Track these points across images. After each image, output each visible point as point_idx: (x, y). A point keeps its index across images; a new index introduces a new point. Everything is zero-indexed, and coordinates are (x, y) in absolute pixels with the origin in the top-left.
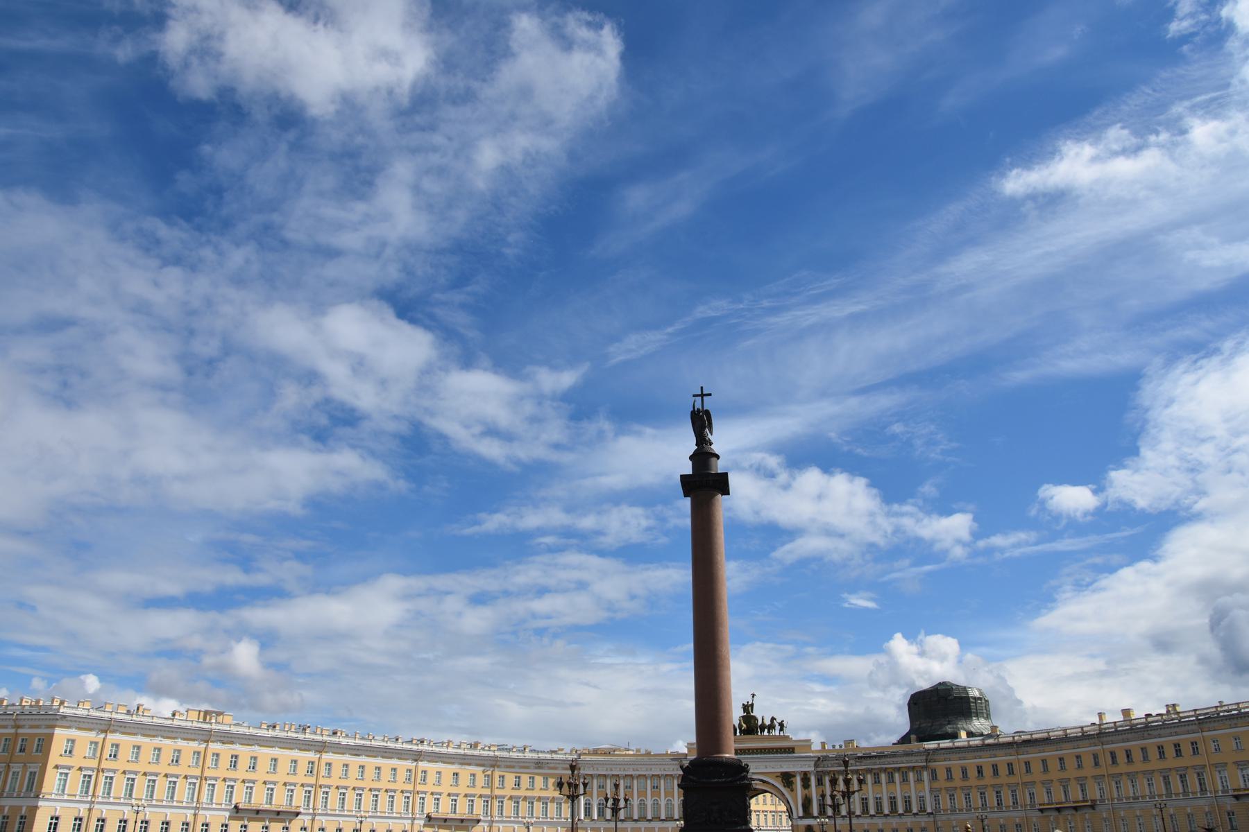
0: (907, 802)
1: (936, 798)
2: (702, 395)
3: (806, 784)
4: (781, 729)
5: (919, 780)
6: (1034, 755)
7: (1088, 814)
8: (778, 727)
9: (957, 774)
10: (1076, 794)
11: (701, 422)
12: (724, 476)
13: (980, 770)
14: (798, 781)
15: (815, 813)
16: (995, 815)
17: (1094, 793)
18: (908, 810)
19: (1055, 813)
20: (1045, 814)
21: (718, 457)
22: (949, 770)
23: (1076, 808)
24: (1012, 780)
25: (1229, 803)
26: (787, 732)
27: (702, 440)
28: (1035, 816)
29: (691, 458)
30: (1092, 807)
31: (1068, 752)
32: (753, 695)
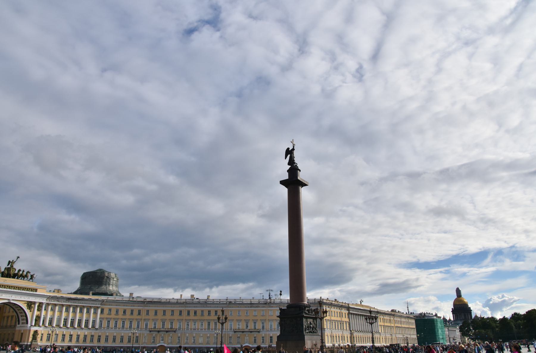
0: (87, 322)
3: (39, 309)
4: (32, 278)
6: (152, 308)
7: (171, 334)
8: (30, 277)
9: (113, 312)
10: (168, 326)
11: (289, 152)
13: (117, 311)
16: (127, 332)
17: (176, 326)
18: (87, 325)
19: (157, 333)
20: (152, 333)
22: (110, 310)
23: (167, 332)
24: (139, 317)
25: (231, 333)
27: (292, 162)
28: (146, 333)
31: (168, 308)
32: (18, 257)
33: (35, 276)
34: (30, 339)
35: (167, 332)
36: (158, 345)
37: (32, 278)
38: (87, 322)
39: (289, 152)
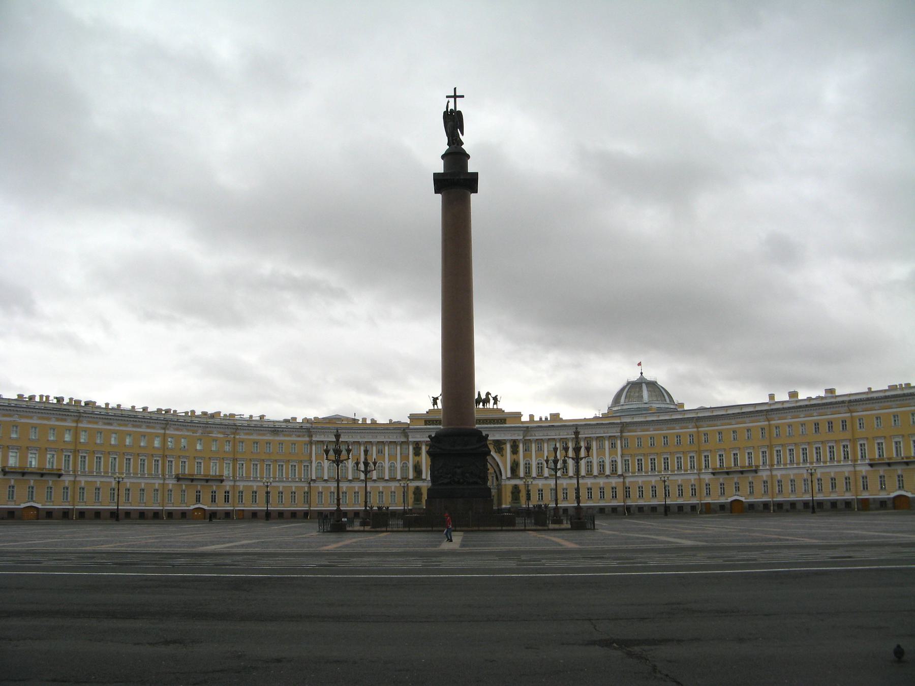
0: (602, 466)
1: (626, 463)
2: (455, 97)
3: (515, 451)
4: (495, 403)
5: (613, 446)
8: (492, 401)
11: (453, 122)
12: (475, 176)
14: (508, 448)
15: (522, 474)
17: (758, 460)
21: (468, 156)
23: (742, 472)
25: (864, 469)
26: (500, 405)
28: (707, 478)
29: (443, 157)
30: (756, 471)
33: (498, 398)
34: (509, 499)
35: (742, 472)
36: (730, 500)
37: (495, 403)
38: (602, 466)
39: (453, 122)
